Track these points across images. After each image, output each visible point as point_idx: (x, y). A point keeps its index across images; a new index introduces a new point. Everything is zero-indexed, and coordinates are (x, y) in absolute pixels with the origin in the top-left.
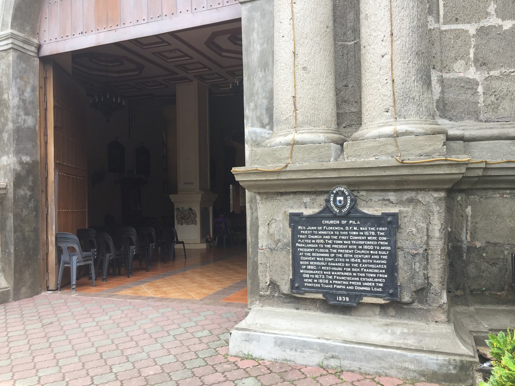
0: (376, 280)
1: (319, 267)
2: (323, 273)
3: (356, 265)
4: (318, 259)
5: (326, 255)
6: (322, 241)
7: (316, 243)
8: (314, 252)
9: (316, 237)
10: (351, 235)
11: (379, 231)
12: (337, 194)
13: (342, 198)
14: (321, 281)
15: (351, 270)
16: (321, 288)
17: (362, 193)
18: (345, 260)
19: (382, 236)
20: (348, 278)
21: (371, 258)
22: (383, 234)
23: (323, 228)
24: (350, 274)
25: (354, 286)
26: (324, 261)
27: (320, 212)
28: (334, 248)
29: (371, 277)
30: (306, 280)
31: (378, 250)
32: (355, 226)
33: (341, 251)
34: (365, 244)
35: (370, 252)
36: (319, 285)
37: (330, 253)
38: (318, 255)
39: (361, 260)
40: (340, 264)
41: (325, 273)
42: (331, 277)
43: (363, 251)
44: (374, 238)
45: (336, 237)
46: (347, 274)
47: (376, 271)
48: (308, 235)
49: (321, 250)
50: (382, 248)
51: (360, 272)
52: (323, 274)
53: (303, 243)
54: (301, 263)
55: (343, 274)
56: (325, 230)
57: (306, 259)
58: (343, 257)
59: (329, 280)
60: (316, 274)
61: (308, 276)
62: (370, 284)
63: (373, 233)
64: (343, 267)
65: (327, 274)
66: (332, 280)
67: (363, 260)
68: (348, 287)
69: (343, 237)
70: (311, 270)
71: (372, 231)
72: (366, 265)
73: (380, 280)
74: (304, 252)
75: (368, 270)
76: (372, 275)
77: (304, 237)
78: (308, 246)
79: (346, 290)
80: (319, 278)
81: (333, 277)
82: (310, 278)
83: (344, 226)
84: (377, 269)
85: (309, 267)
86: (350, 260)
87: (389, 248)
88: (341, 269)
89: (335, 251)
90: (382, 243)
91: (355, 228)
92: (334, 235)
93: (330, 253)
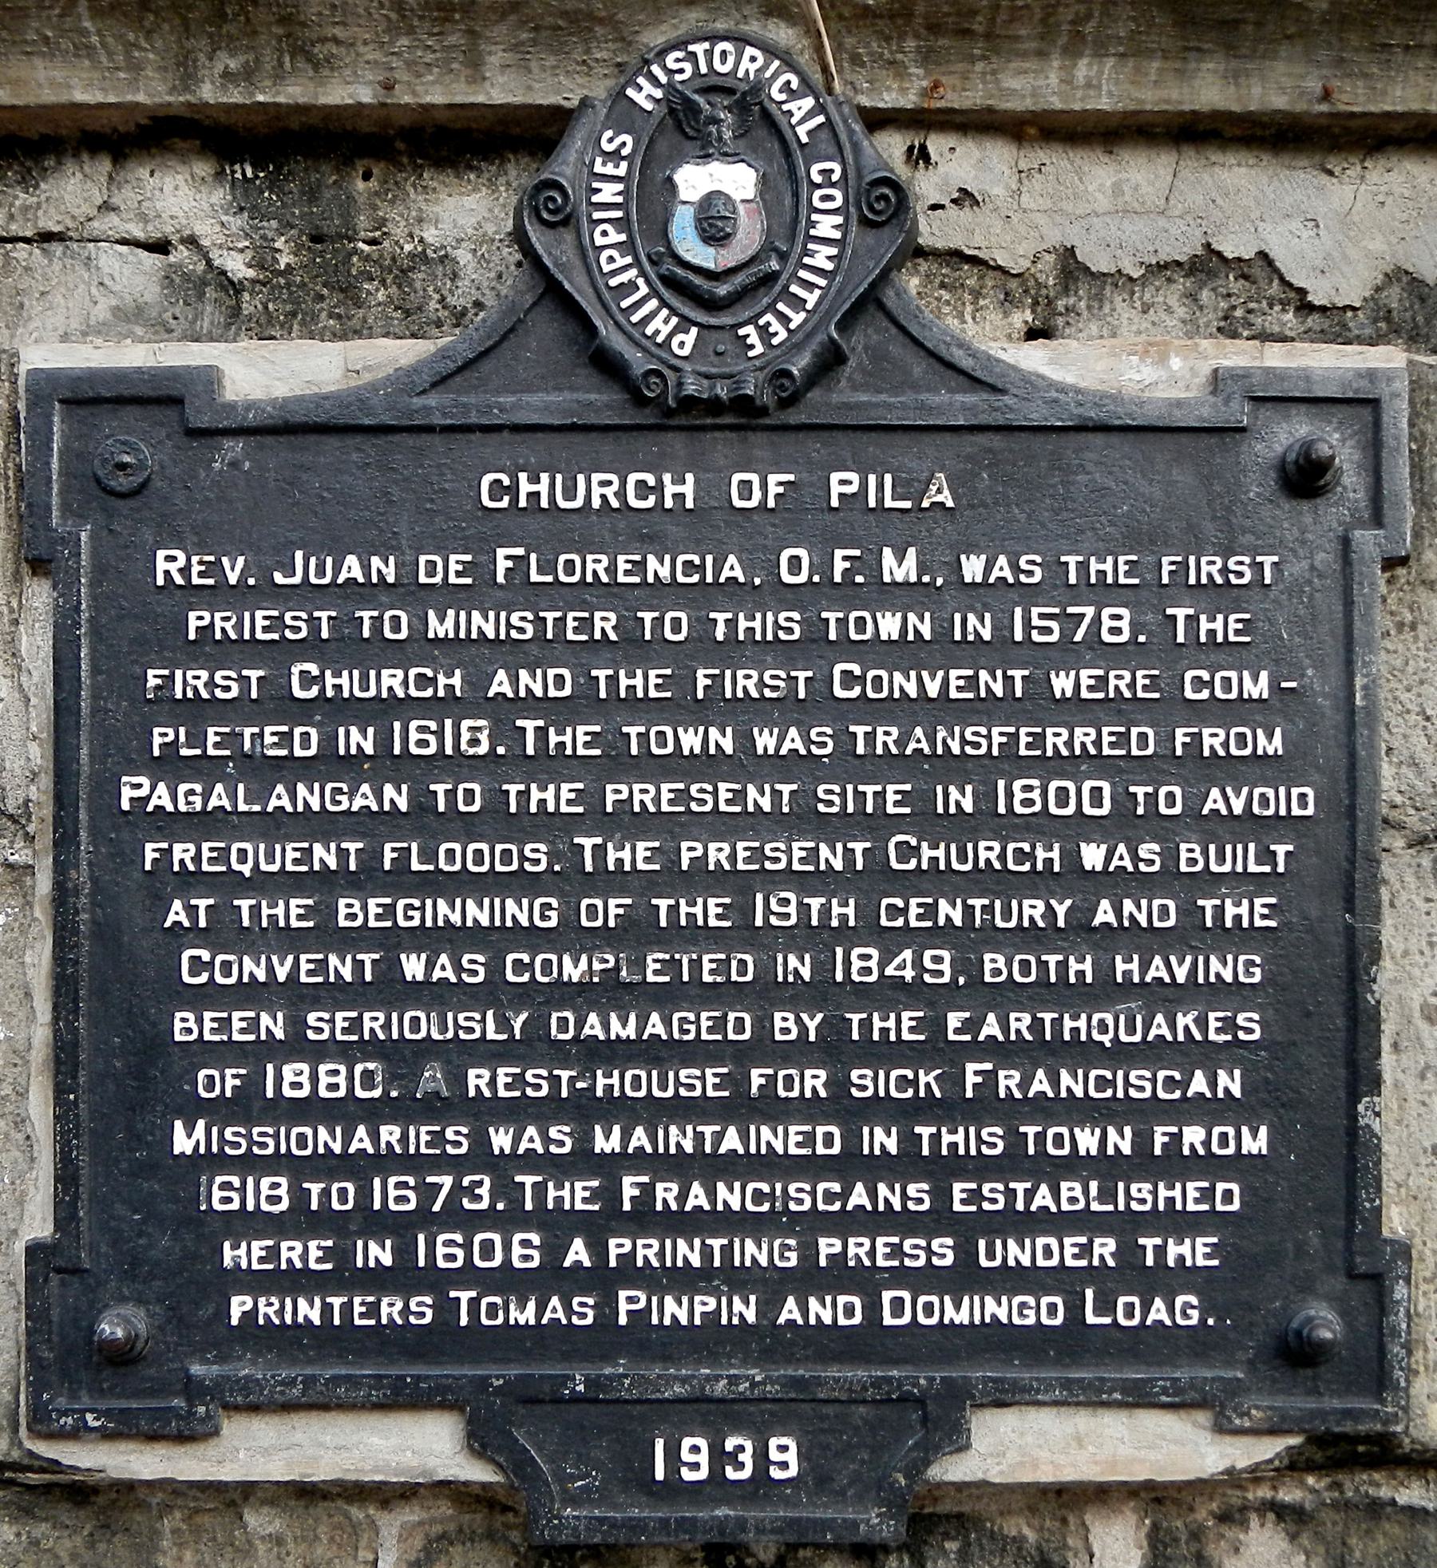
0: (1141, 1194)
1: (432, 1078)
2: (481, 1141)
3: (906, 1024)
4: (413, 967)
5: (517, 911)
6: (474, 735)
7: (389, 764)
8: (365, 879)
9: (391, 680)
10: (847, 648)
11: (1181, 587)
12: (685, 125)
13: (737, 180)
14: (446, 1250)
15: (839, 1085)
16: (445, 1338)
17: (959, 162)
18: (765, 970)
19: (1217, 651)
20: (801, 1196)
21: (1081, 932)
22: (1223, 626)
23: (480, 569)
24: (828, 1138)
25: (866, 1281)
26: (493, 994)
27: (445, 376)
28: (629, 823)
29: (1075, 1165)
30: (244, 1254)
31: (1166, 830)
32: (899, 528)
33: (717, 853)
34: (1010, 762)
35: (1072, 858)
36: (423, 1308)
37: (571, 880)
38: (409, 913)
39: (968, 965)
40: (697, 1024)
41: (501, 1140)
42: (578, 1195)
43: (988, 851)
44: (1119, 681)
45: (646, 682)
46: (786, 1139)
47: (1141, 1083)
48: (279, 653)
49: (456, 855)
50: (1214, 801)
51: (949, 1108)
52: (481, 1157)
53: (205, 769)
54: (184, 1025)
55: (732, 1141)
56: (522, 591)
57: (253, 968)
58: (743, 932)
59: (557, 1226)
60: (385, 1162)
61: (272, 1193)
62: (1068, 1251)
63: (1117, 623)
64: (742, 1056)
65: (529, 1161)
66: (594, 1229)
67: (993, 962)
68: (790, 1311)
69: (745, 682)
70: (312, 1110)
71: (1104, 592)
72: (1020, 1022)
73: (1189, 1195)
74: (230, 884)
75: (1040, 1084)
76: (1087, 1141)
77: (227, 685)
78: (279, 799)
79: (767, 1341)
80: (424, 1219)
81: (610, 1194)
82: (301, 1220)
83: (755, 533)
84: (1152, 1053)
85: (293, 1078)
86: (823, 967)
87: (1300, 800)
88: (708, 1081)
89: (639, 854)
90: (1212, 739)
91: (898, 568)
92: (633, 647)
93: (571, 880)
